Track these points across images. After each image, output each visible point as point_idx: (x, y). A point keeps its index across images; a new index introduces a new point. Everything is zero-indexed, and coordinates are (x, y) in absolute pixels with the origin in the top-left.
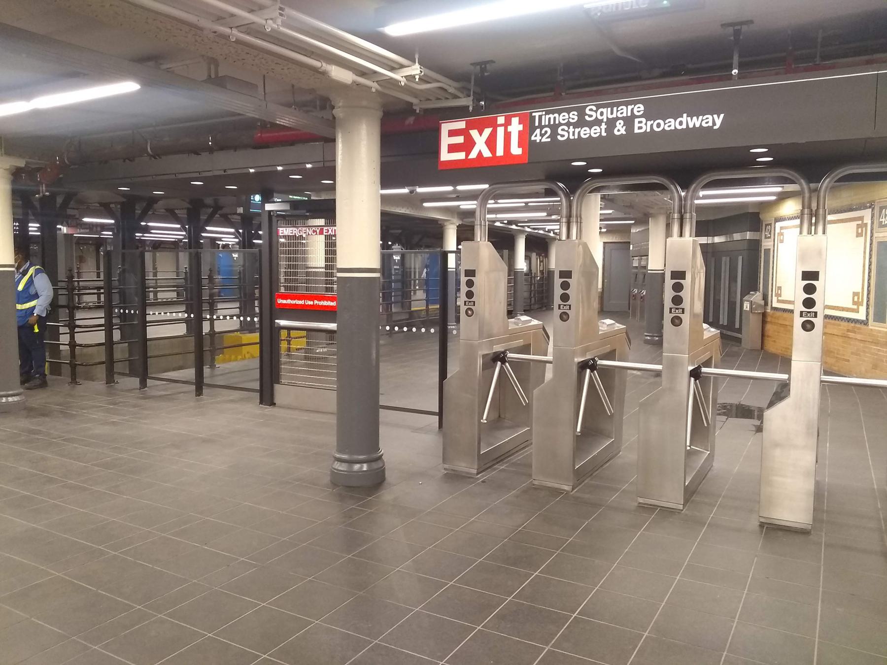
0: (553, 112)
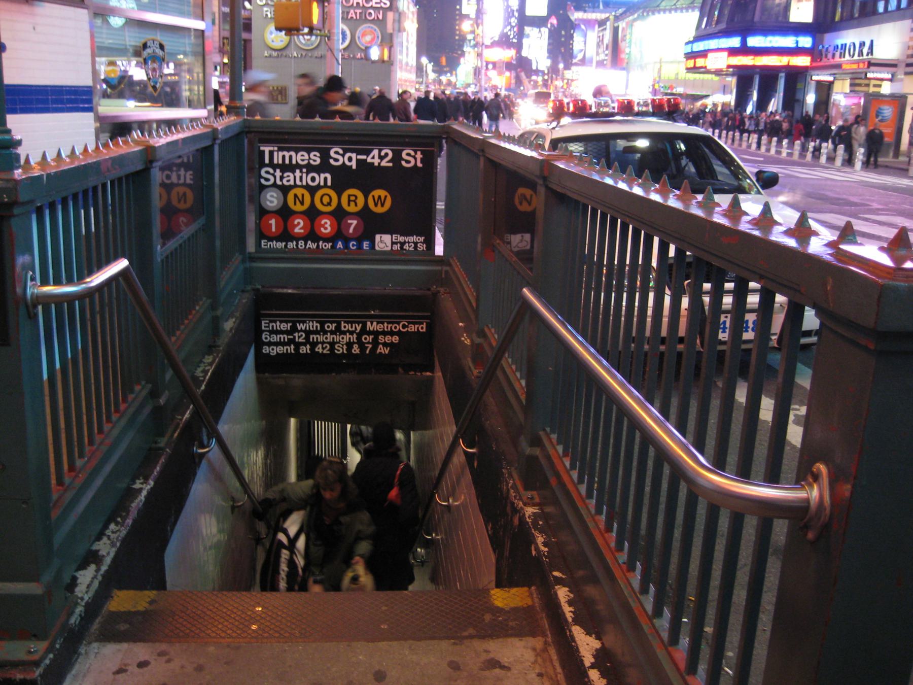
0: (288, 150)
